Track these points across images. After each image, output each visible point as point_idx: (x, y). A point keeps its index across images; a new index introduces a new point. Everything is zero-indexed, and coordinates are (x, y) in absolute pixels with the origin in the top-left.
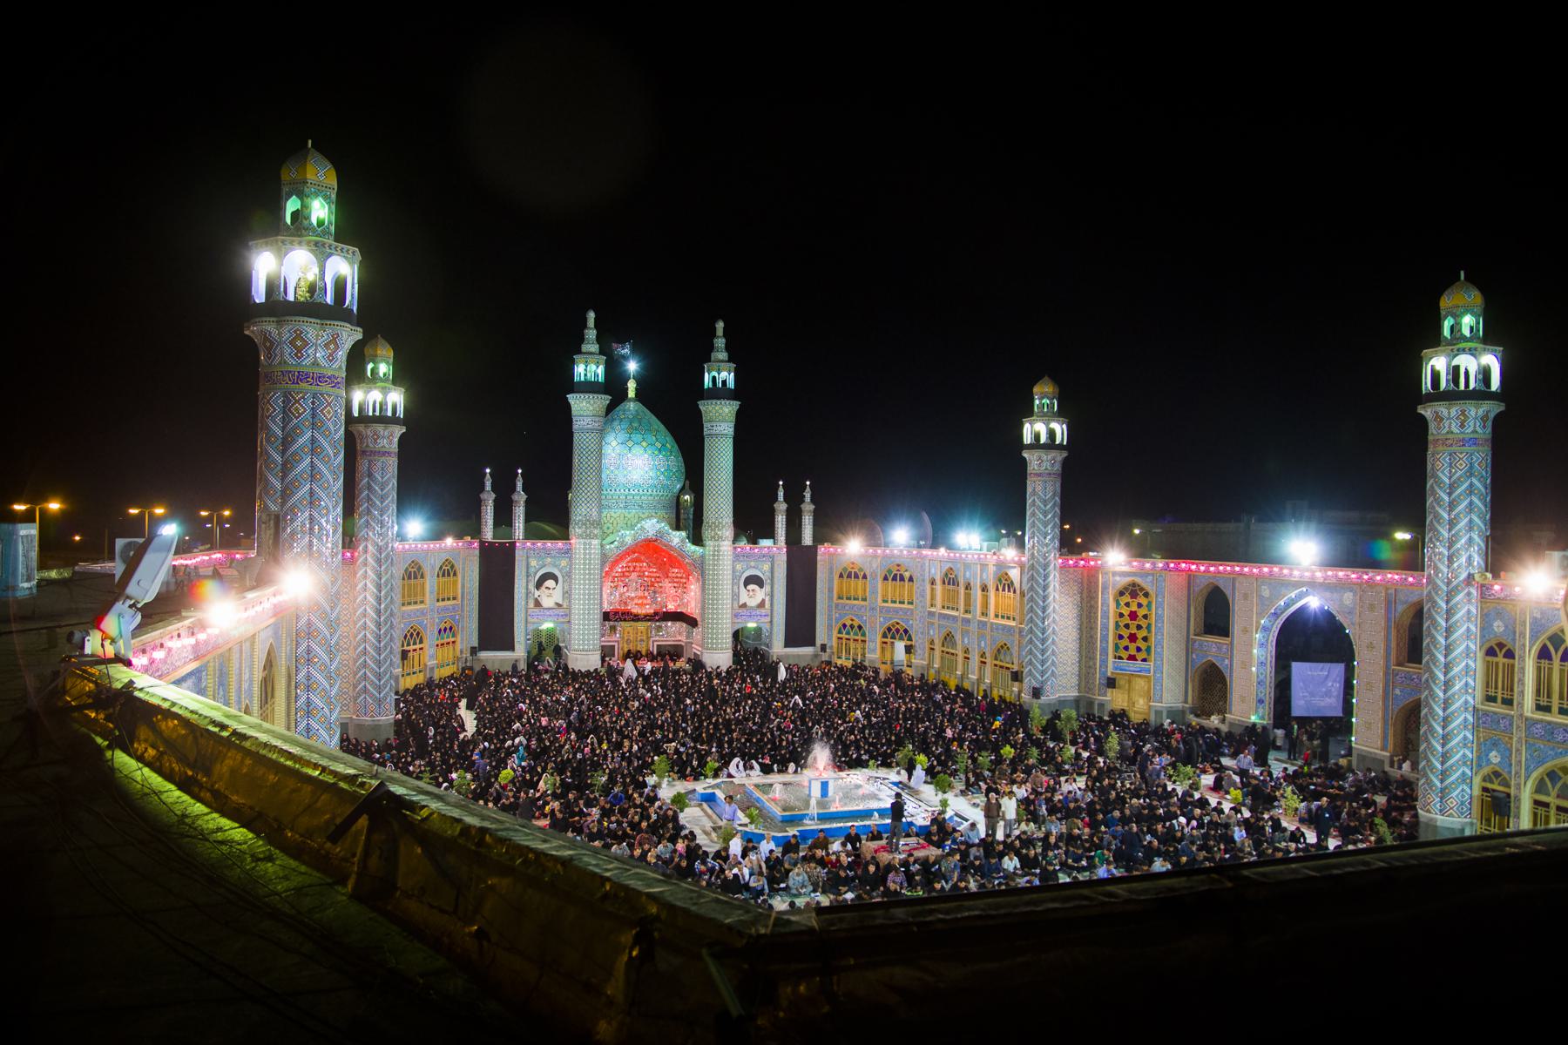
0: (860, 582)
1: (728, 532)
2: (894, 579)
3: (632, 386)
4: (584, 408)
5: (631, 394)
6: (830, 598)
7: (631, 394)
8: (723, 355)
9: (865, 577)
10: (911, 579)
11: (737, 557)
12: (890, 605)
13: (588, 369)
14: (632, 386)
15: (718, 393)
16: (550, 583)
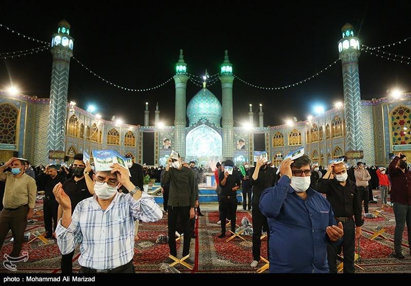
0: (281, 138)
1: (232, 123)
2: (294, 135)
3: (204, 84)
4: (180, 84)
5: (204, 86)
6: (271, 147)
7: (204, 86)
8: (227, 61)
9: (283, 136)
10: (300, 134)
11: (235, 131)
12: (292, 145)
13: (181, 68)
14: (204, 84)
15: (224, 74)
16: (167, 141)
